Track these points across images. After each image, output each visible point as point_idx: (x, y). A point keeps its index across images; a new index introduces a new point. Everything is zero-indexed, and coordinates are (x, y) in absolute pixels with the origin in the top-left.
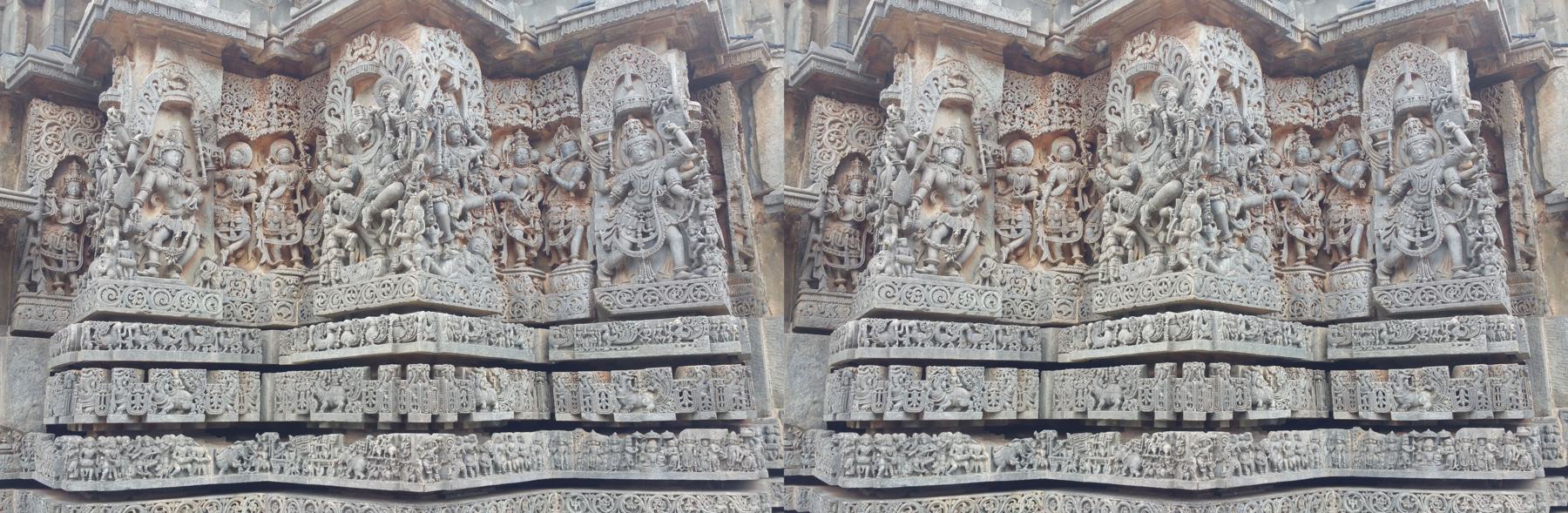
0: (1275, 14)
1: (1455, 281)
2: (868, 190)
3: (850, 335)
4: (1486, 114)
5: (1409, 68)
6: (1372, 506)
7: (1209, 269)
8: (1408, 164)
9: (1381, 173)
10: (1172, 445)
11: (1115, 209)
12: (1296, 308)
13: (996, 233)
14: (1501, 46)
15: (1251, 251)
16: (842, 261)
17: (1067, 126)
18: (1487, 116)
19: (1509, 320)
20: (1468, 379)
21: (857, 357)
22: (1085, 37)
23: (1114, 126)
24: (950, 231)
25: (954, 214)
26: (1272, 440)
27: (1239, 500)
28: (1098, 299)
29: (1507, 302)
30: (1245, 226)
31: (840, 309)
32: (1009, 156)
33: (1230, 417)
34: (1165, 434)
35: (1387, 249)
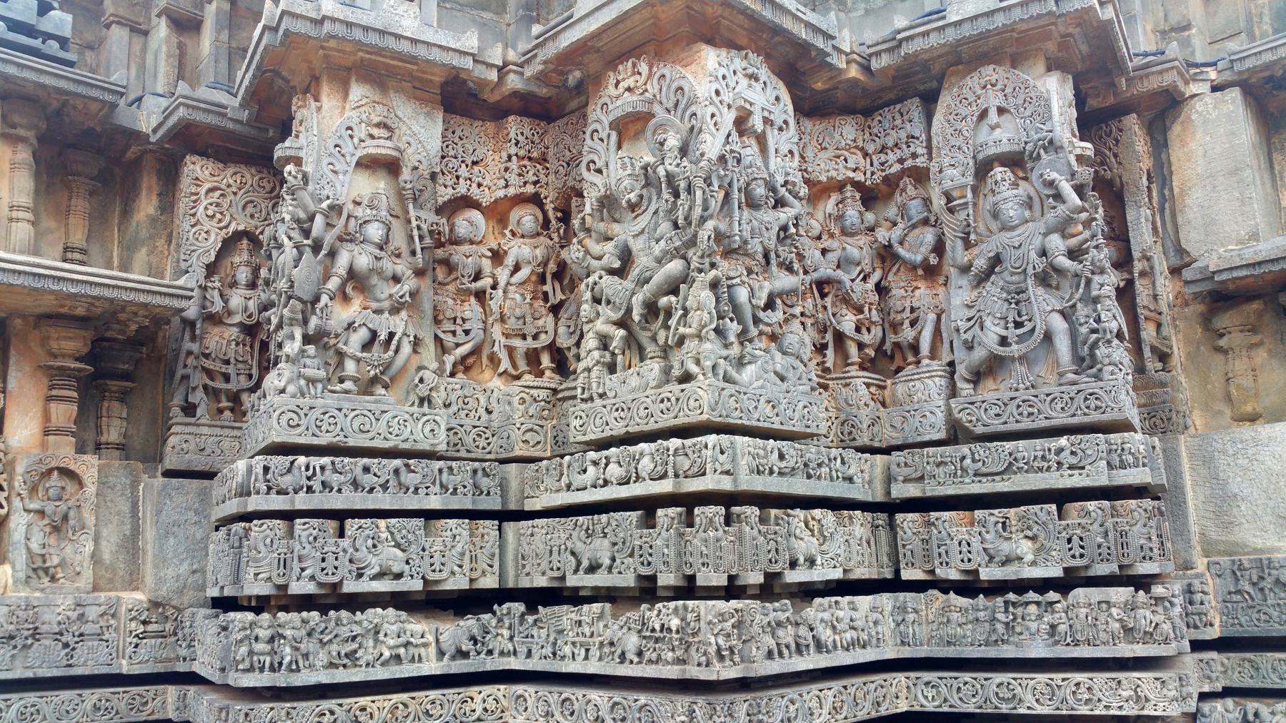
0: (810, 31)
1: (1063, 388)
2: (260, 282)
3: (240, 479)
4: (1100, 160)
5: (993, 100)
6: (956, 697)
7: (727, 379)
8: (997, 231)
9: (959, 243)
10: (682, 620)
11: (597, 301)
12: (847, 429)
13: (436, 337)
14: (1120, 68)
15: (784, 353)
16: (227, 378)
17: (530, 189)
18: (1102, 164)
19: (1137, 441)
20: (1083, 521)
21: (250, 509)
22: (552, 67)
23: (594, 187)
24: (374, 334)
25: (378, 312)
26: (818, 610)
27: (774, 692)
28: (577, 423)
29: (1134, 415)
30: (775, 320)
31: (226, 444)
32: (451, 230)
33: (761, 580)
34: (672, 604)
35: (969, 347)
